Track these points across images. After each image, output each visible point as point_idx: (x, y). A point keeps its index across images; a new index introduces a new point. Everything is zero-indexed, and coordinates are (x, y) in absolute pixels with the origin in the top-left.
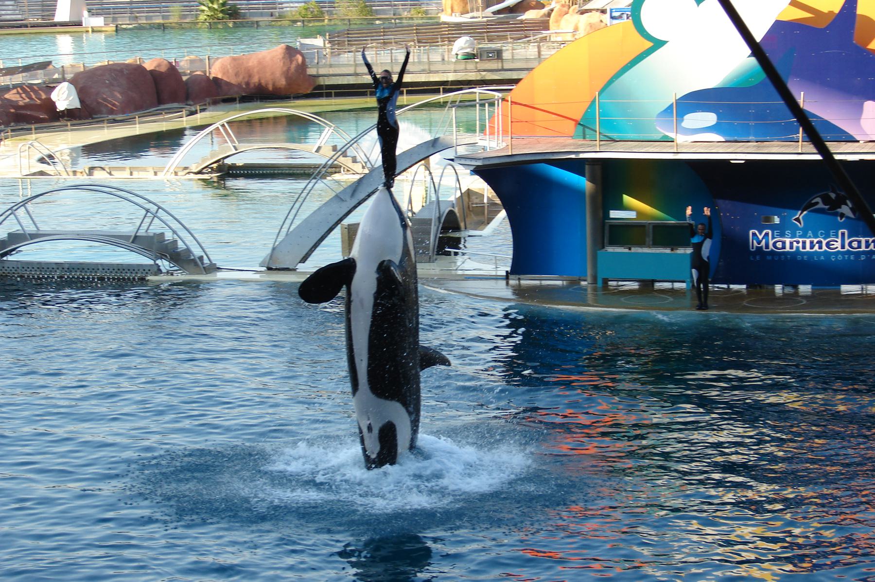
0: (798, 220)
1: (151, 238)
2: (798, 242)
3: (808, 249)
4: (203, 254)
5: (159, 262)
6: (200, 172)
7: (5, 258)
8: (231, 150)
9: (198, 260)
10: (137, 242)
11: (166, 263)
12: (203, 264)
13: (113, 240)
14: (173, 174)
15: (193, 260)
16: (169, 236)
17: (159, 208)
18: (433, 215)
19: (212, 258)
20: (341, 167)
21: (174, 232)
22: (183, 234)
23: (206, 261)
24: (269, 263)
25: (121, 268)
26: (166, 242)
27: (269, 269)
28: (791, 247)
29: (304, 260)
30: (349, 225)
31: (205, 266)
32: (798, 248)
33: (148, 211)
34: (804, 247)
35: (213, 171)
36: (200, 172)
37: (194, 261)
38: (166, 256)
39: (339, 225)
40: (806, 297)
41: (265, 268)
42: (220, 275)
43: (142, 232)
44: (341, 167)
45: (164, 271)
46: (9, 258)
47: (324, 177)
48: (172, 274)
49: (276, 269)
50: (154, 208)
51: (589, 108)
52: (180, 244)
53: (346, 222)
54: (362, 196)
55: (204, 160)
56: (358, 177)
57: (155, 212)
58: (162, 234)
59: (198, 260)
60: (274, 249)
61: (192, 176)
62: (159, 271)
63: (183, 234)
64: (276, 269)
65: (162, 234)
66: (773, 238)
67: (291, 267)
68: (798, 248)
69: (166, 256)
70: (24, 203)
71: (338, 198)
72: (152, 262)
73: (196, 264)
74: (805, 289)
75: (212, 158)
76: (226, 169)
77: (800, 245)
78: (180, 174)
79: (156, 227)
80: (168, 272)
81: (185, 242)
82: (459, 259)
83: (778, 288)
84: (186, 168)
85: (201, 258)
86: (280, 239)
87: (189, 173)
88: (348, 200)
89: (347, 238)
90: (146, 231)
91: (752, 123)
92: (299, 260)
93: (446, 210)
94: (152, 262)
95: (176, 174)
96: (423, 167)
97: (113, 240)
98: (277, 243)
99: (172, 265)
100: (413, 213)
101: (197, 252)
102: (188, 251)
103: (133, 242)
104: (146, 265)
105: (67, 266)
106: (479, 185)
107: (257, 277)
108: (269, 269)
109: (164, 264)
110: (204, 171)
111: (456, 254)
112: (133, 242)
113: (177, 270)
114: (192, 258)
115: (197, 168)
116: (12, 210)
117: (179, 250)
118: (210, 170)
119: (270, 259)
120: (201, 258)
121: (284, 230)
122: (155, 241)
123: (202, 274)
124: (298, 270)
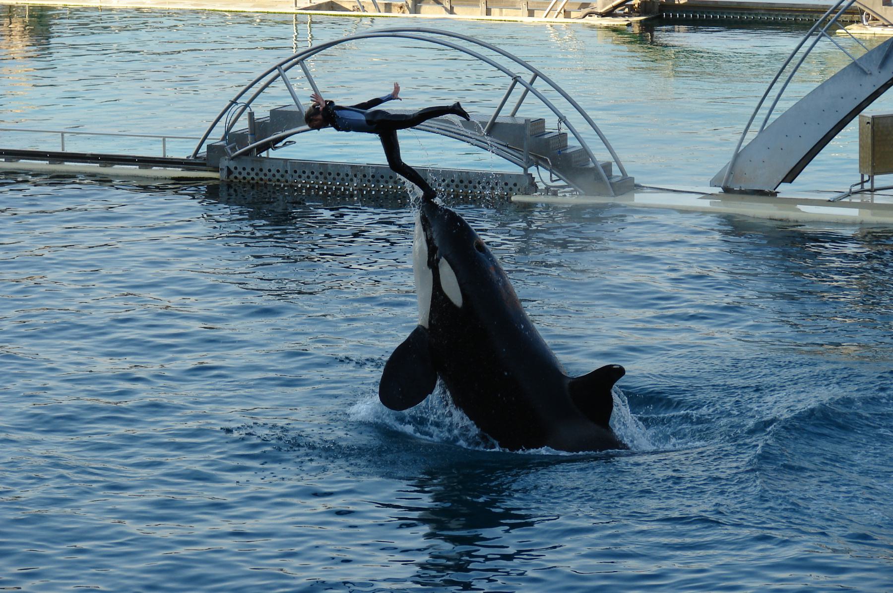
1: (522, 127)
4: (611, 160)
5: (532, 170)
6: (610, 13)
7: (264, 154)
9: (602, 171)
12: (610, 176)
14: (562, 15)
15: (593, 169)
16: (551, 124)
17: (537, 74)
19: (627, 168)
20: (862, 12)
21: (562, 119)
22: (573, 117)
24: (727, 180)
26: (546, 137)
27: (727, 190)
29: (791, 177)
30: (873, 118)
31: (614, 180)
33: (516, 80)
36: (610, 13)
37: (594, 170)
38: (545, 161)
39: (856, 120)
41: (720, 190)
42: (640, 199)
43: (504, 116)
44: (862, 12)
45: (541, 186)
46: (272, 154)
47: (831, 32)
48: (555, 194)
50: (527, 76)
52: (572, 143)
53: (870, 111)
57: (528, 82)
58: (541, 122)
59: (602, 171)
60: (737, 156)
61: (595, 20)
62: (532, 186)
63: (573, 117)
65: (541, 122)
69: (545, 161)
70: (301, 59)
71: (857, 68)
72: (519, 171)
73: (598, 178)
76: (656, 9)
78: (573, 14)
79: (532, 110)
80: (548, 189)
84: (584, 5)
86: (751, 136)
87: (590, 14)
88: (875, 71)
89: (869, 141)
90: (513, 115)
94: (519, 171)
95: (567, 14)
98: (741, 148)
99: (554, 177)
101: (601, 155)
102: (585, 153)
104: (510, 176)
105: (371, 172)
107: (706, 204)
109: (542, 176)
110: (617, 11)
113: (563, 187)
114: (592, 165)
115: (604, 6)
116: (280, 70)
117: (569, 151)
118: (627, 10)
119: (731, 173)
120: (607, 167)
121: (756, 127)
122: (528, 132)
123: (608, 195)
124: (779, 196)
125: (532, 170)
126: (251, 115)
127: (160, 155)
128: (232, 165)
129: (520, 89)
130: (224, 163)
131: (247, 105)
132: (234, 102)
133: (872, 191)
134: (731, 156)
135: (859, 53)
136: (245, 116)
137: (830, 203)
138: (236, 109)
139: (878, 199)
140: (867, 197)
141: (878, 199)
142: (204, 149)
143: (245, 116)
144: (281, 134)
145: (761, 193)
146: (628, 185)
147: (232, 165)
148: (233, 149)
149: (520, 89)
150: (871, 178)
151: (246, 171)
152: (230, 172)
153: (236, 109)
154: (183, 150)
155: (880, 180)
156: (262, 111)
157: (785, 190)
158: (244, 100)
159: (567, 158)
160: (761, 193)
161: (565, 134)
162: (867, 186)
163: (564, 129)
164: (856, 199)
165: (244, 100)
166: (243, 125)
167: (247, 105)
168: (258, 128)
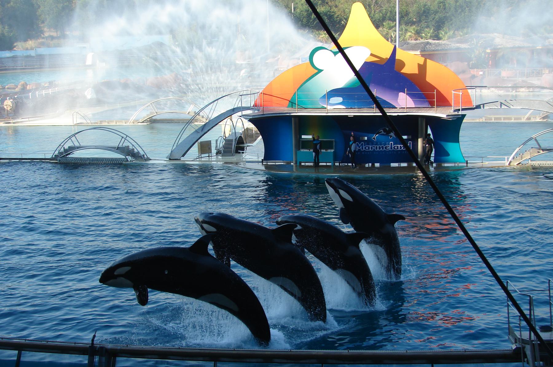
0: (374, 138)
1: (124, 148)
2: (374, 147)
3: (378, 149)
5: (127, 157)
6: (143, 122)
7: (67, 156)
10: (119, 149)
11: (130, 157)
12: (144, 157)
13: (109, 148)
16: (131, 147)
17: (127, 136)
18: (234, 138)
19: (148, 156)
20: (197, 120)
21: (133, 145)
22: (136, 146)
23: (145, 156)
25: (112, 159)
27: (170, 159)
28: (372, 149)
29: (183, 156)
32: (374, 149)
33: (123, 137)
34: (377, 149)
35: (148, 121)
36: (143, 122)
40: (377, 168)
42: (151, 162)
43: (120, 145)
44: (197, 120)
45: (129, 160)
46: (69, 156)
49: (173, 159)
50: (125, 136)
51: (293, 96)
52: (135, 150)
53: (199, 141)
54: (206, 131)
55: (144, 118)
56: (204, 123)
60: (172, 152)
61: (140, 124)
63: (136, 146)
64: (173, 159)
66: (365, 145)
67: (178, 159)
68: (374, 149)
70: (74, 135)
71: (197, 131)
72: (124, 157)
73: (142, 158)
74: (377, 165)
75: (147, 117)
77: (375, 148)
79: (126, 144)
80: (131, 161)
81: (137, 149)
83: (367, 165)
85: (144, 155)
86: (174, 147)
87: (139, 122)
88: (200, 132)
91: (356, 101)
92: (181, 156)
93: (238, 136)
94: (124, 157)
95: (133, 123)
96: (229, 119)
97: (109, 148)
100: (226, 137)
101: (142, 153)
102: (138, 153)
103: (117, 149)
104: (122, 158)
105: (91, 159)
106: (251, 126)
107: (165, 162)
108: (170, 159)
111: (243, 153)
112: (117, 149)
116: (70, 138)
120: (144, 155)
121: (176, 145)
125: (127, 157)
126: (64, 148)
127: (44, 157)
128: (60, 159)
129: (123, 139)
130: (59, 159)
131: (63, 146)
132: (60, 145)
134: (170, 152)
135: (197, 128)
136: (63, 148)
137: (192, 161)
138: (61, 147)
139: (203, 160)
140: (200, 159)
141: (203, 160)
142: (54, 156)
143: (63, 148)
144: (71, 152)
145: (177, 159)
147: (60, 159)
148: (60, 156)
149: (123, 139)
150: (201, 155)
151: (63, 160)
152: (60, 161)
153: (61, 147)
154: (49, 156)
155: (203, 155)
156: (66, 147)
157: (182, 159)
158: (62, 144)
159: (135, 154)
160: (177, 159)
161: (134, 149)
162: (200, 157)
163: (134, 147)
164: (198, 160)
165: (62, 144)
166: (62, 149)
167: (63, 146)
168: (66, 151)
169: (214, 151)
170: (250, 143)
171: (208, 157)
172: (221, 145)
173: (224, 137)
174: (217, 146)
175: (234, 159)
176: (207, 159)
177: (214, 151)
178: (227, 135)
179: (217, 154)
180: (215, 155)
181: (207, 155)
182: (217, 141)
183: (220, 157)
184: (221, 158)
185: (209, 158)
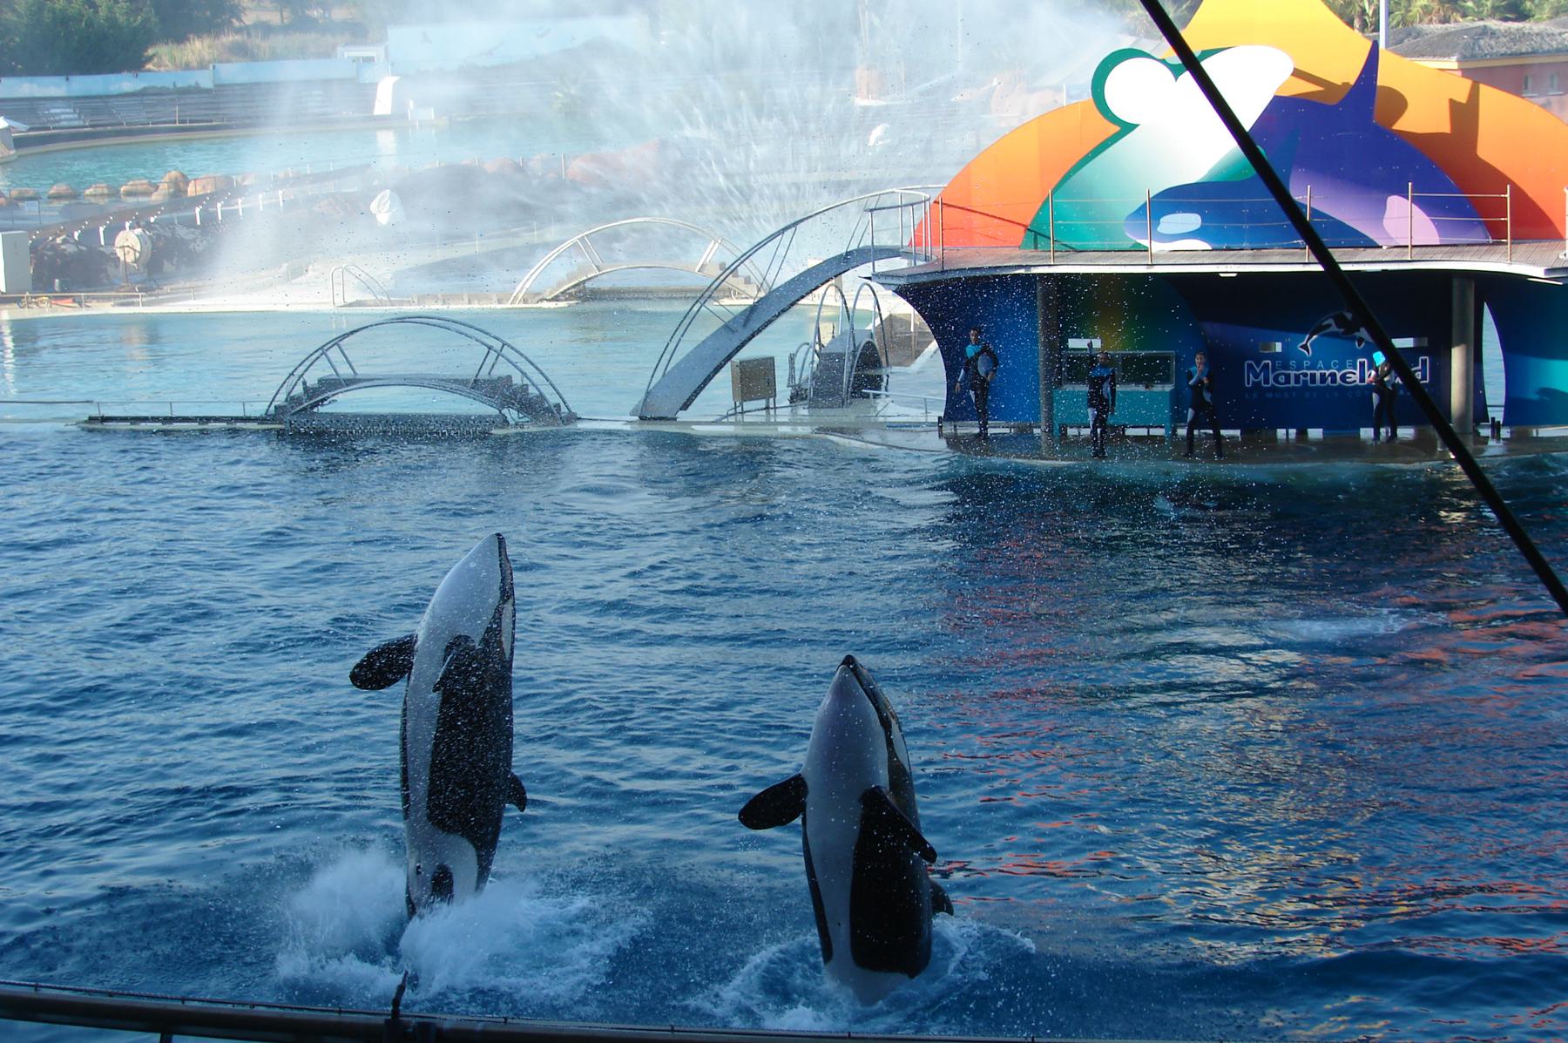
8: (592, 271)
18: (847, 348)
23: (564, 409)
27: (641, 418)
29: (685, 406)
36: (556, 299)
39: (729, 364)
42: (581, 426)
51: (1040, 210)
53: (737, 358)
54: (756, 326)
56: (751, 302)
61: (545, 305)
82: (880, 403)
87: (541, 300)
88: (740, 329)
93: (862, 341)
96: (832, 291)
100: (822, 346)
106: (903, 308)
107: (628, 428)
111: (876, 396)
133: (743, 413)
140: (739, 417)
141: (747, 418)
146: (573, 418)
150: (741, 404)
155: (748, 405)
164: (732, 419)
169: (783, 391)
170: (900, 364)
171: (764, 412)
172: (807, 373)
173: (817, 347)
174: (792, 377)
175: (846, 415)
176: (760, 416)
177: (783, 391)
178: (826, 339)
179: (792, 400)
180: (788, 403)
181: (762, 403)
182: (792, 359)
183: (803, 411)
184: (806, 412)
185: (768, 413)
